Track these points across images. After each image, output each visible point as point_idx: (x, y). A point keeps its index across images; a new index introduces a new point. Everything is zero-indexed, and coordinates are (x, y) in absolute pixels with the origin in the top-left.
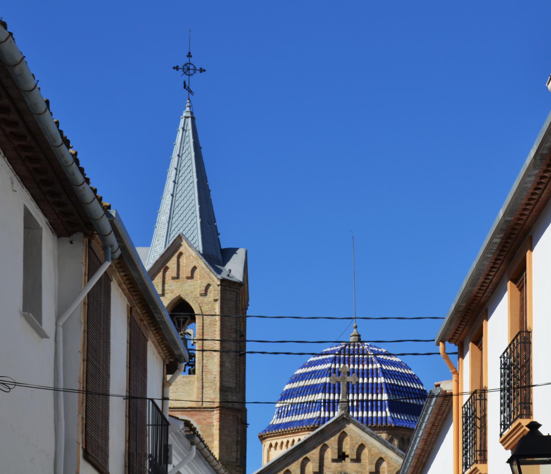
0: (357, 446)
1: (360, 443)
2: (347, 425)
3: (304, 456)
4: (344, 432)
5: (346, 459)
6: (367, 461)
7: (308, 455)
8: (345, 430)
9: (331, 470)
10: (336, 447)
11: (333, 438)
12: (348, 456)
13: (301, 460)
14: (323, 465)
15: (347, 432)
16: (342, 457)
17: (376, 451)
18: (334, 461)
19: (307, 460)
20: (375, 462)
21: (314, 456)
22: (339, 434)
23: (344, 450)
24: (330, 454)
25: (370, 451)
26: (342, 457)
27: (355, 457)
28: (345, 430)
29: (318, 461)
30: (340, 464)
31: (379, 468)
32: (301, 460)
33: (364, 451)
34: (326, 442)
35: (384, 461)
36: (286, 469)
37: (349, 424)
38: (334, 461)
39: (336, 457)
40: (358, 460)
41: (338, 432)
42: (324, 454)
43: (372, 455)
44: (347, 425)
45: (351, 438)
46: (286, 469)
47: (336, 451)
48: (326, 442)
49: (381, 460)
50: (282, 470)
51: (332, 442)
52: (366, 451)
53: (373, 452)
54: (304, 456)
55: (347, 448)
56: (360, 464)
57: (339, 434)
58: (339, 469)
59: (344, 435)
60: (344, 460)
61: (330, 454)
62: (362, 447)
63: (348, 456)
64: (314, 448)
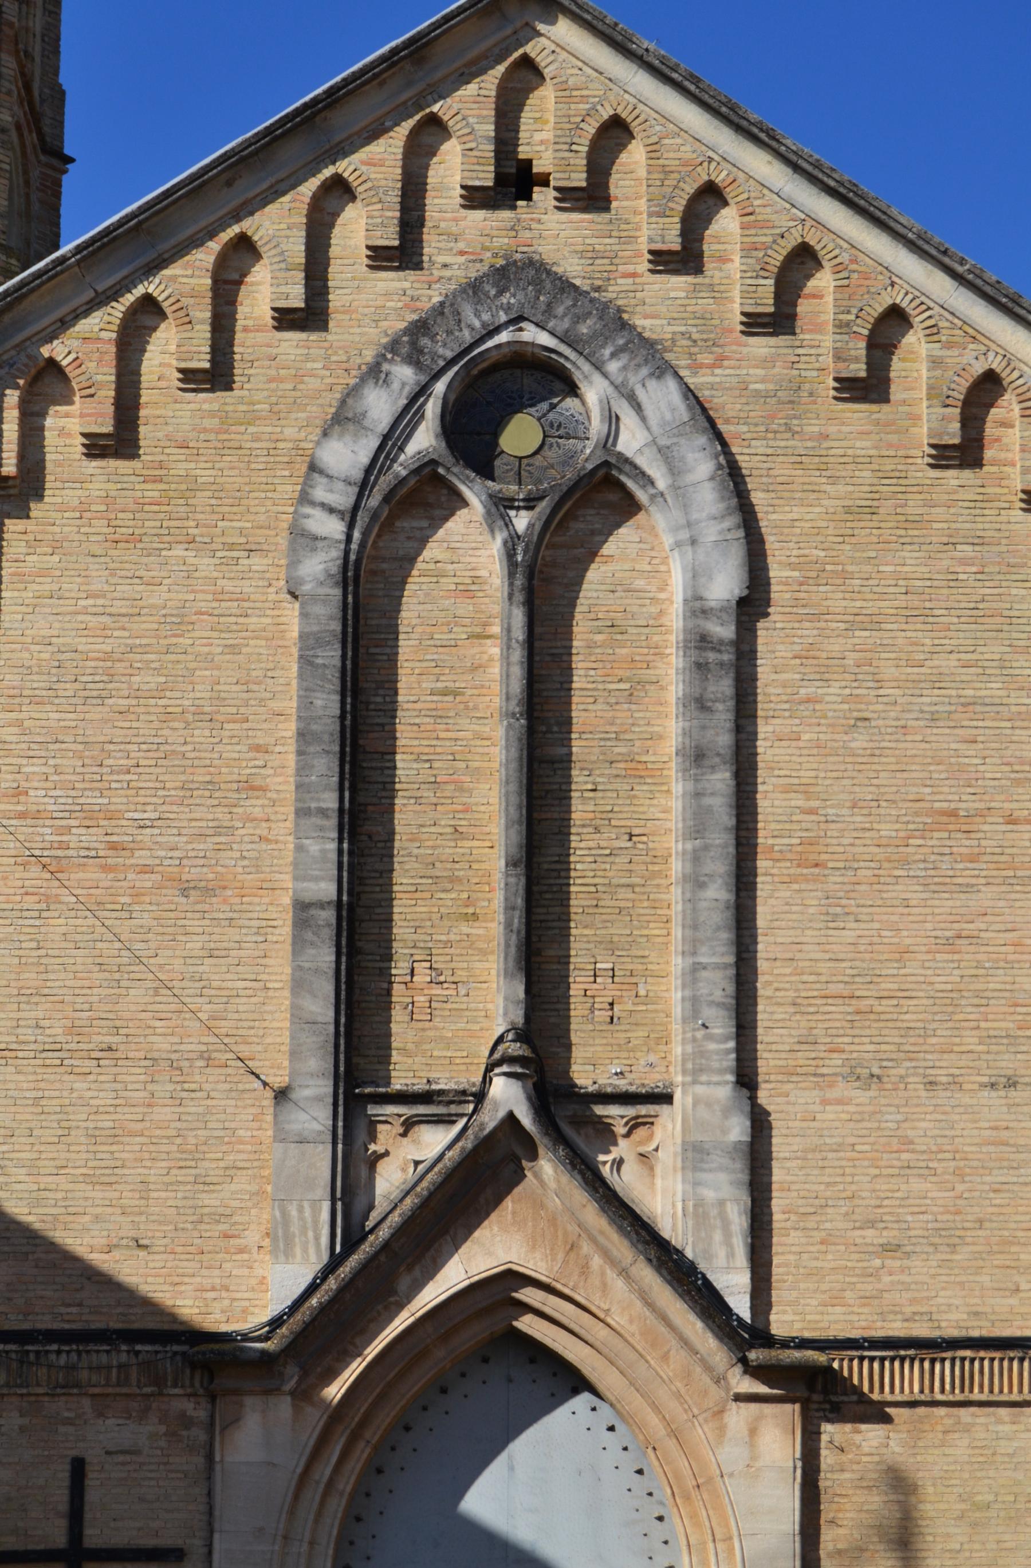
0: (591, 128)
1: (606, 113)
2: (541, 27)
3: (328, 172)
4: (527, 63)
5: (539, 193)
6: (642, 204)
7: (344, 167)
8: (530, 49)
9: (461, 245)
10: (489, 129)
11: (471, 89)
12: (544, 181)
13: (310, 187)
14: (421, 222)
15: (541, 61)
16: (513, 182)
17: (687, 152)
18: (475, 198)
19: (340, 190)
20: (679, 205)
21: (374, 173)
22: (501, 69)
23: (524, 152)
24: (457, 165)
25: (654, 151)
26: (513, 182)
27: (579, 179)
28: (530, 49)
29: (394, 197)
30: (506, 214)
31: (701, 240)
32: (310, 187)
33: (623, 157)
34: (435, 108)
35: (726, 203)
36: (235, 229)
37: (553, 22)
38: (475, 198)
39: (486, 178)
40: (591, 196)
41: (499, 61)
42: (427, 167)
43: (666, 172)
44: (541, 27)
45: (563, 87)
46: (235, 229)
47: (488, 149)
48: (435, 108)
49: (711, 201)
50: (212, 235)
51: (469, 107)
52: (634, 157)
53: (670, 158)
54: (328, 172)
55: (547, 137)
56: (605, 217)
57: (501, 69)
58: (503, 242)
59: (527, 74)
60: (529, 198)
61: (457, 165)
62: (615, 132)
63: (544, 181)
64: (375, 132)
